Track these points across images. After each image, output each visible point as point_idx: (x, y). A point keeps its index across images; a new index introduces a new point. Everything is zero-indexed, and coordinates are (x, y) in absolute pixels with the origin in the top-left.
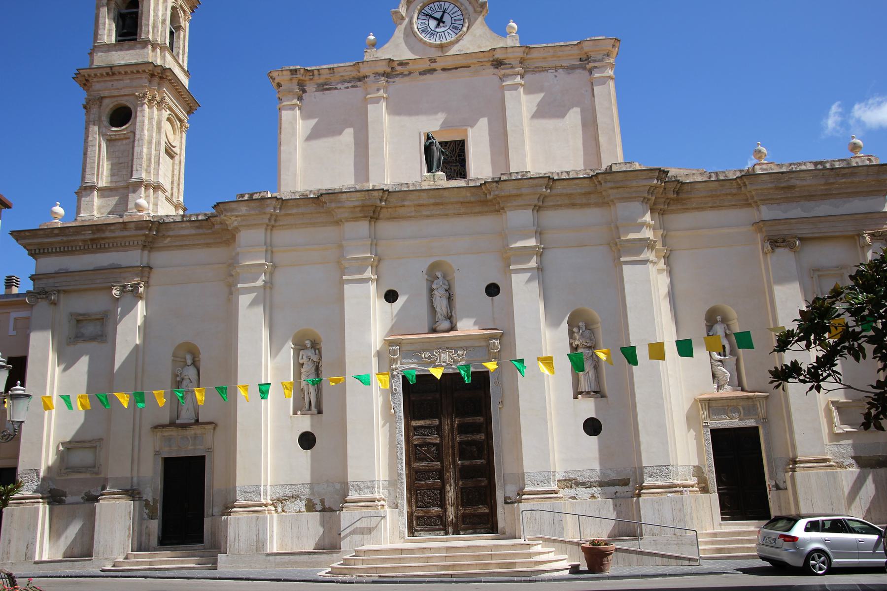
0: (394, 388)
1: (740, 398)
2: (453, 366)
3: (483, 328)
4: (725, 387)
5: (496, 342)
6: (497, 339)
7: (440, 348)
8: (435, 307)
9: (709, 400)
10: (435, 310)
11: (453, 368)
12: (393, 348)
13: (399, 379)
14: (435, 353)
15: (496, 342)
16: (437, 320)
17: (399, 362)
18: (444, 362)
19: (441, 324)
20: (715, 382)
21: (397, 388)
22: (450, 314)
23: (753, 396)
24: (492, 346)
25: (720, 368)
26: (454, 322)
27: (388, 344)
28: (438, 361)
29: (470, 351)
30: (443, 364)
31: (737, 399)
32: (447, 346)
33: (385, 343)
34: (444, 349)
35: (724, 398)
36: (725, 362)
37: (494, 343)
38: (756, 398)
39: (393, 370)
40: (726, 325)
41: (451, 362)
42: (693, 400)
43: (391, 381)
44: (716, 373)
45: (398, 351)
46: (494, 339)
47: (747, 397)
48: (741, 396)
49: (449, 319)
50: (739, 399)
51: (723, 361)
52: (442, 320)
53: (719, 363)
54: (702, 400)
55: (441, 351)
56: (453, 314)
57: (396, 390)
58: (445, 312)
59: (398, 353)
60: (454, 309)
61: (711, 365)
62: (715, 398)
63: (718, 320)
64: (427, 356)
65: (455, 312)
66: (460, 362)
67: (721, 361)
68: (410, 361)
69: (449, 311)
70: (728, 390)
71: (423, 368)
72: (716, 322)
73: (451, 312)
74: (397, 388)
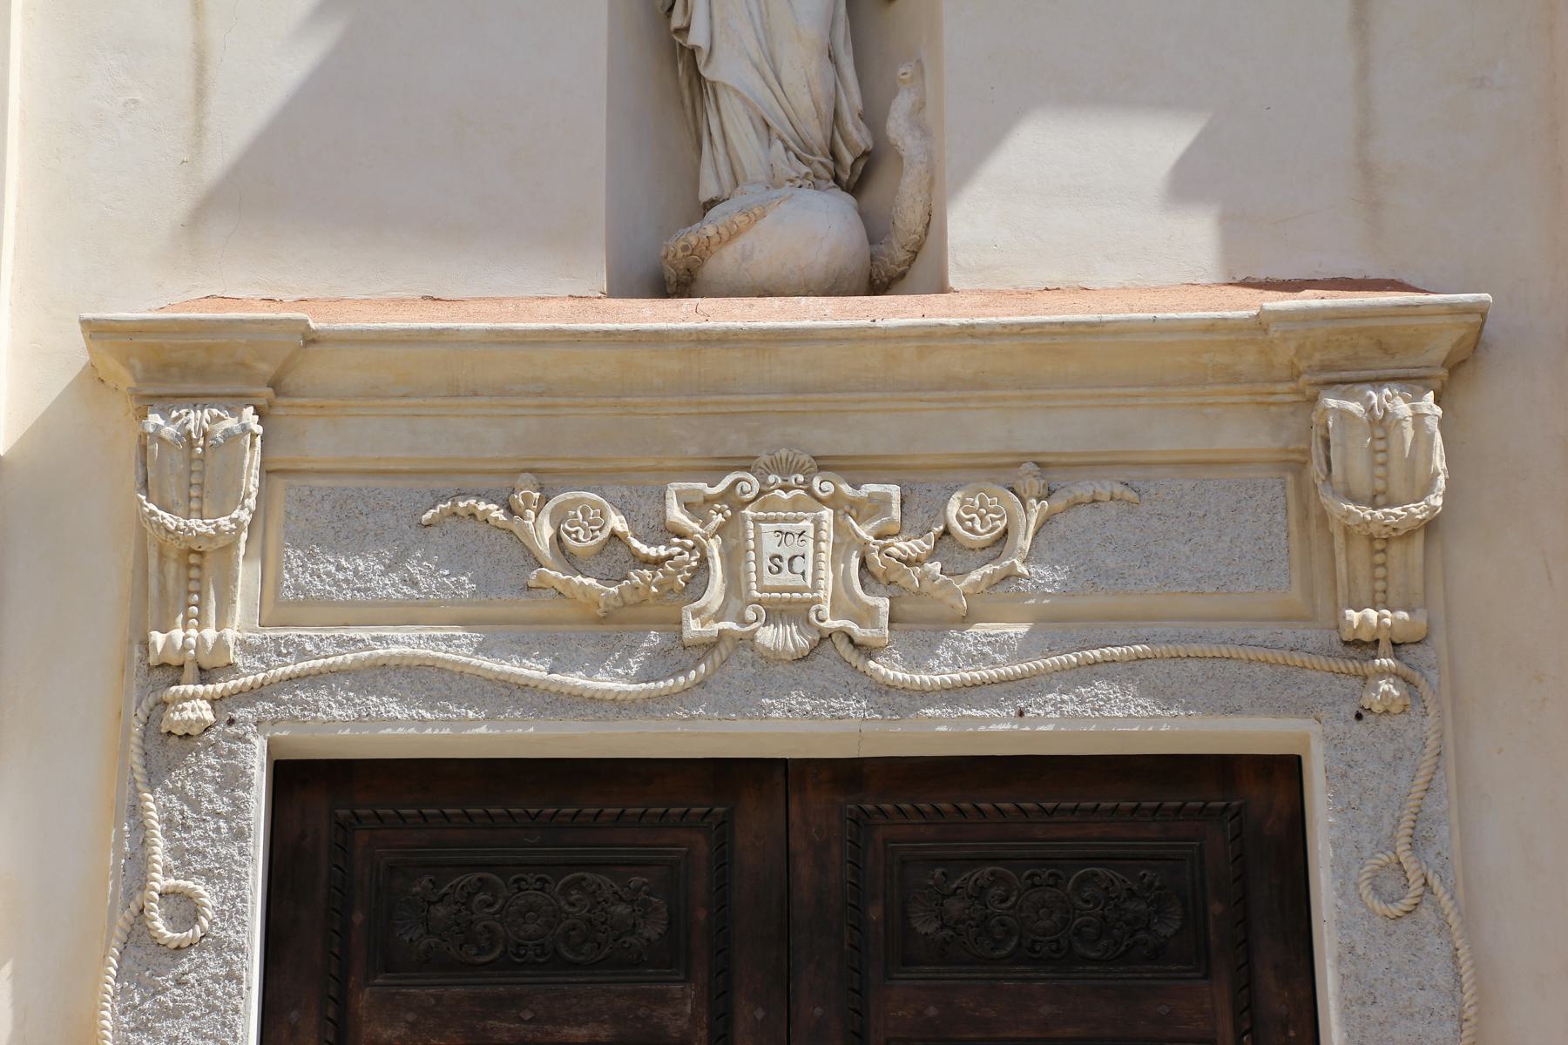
0: (160, 882)
2: (887, 669)
3: (1261, 276)
5: (1402, 408)
6: (1411, 381)
7: (745, 464)
8: (697, 37)
10: (697, 80)
11: (885, 689)
12: (195, 419)
13: (233, 779)
14: (676, 514)
15: (1402, 408)
16: (709, 190)
17: (247, 576)
18: (776, 613)
19: (754, 219)
21: (199, 887)
22: (860, 137)
24: (1354, 461)
26: (909, 216)
27: (127, 380)
28: (715, 594)
29: (1084, 515)
30: (768, 636)
32: (827, 439)
33: (93, 378)
34: (785, 468)
37: (1382, 424)
39: (172, 671)
41: (866, 616)
43: (136, 810)
45: (252, 460)
46: (1378, 382)
49: (855, 188)
52: (774, 183)
55: (750, 485)
56: (897, 126)
57: (184, 907)
58: (803, 102)
59: (252, 482)
60: (905, 70)
64: (583, 542)
65: (920, 106)
66: (967, 619)
68: (389, 587)
69: (852, 101)
71: (533, 670)
73: (873, 117)
74: (199, 887)
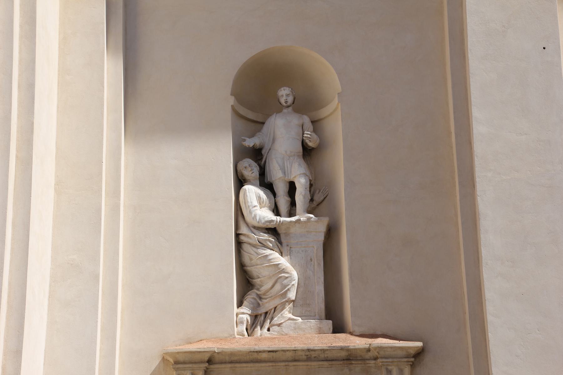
1: (322, 356)
4: (276, 320)
9: (210, 361)
20: (245, 303)
23: (369, 350)
25: (268, 252)
31: (309, 359)
35: (264, 356)
36: (287, 234)
38: (376, 359)
40: (306, 120)
42: (156, 362)
44: (254, 270)
47: (344, 354)
48: (323, 351)
50: (317, 359)
51: (281, 231)
53: (265, 236)
54: (181, 358)
61: (239, 244)
62: (232, 354)
63: (283, 101)
67: (273, 231)
70: (285, 330)
72: (279, 108)
